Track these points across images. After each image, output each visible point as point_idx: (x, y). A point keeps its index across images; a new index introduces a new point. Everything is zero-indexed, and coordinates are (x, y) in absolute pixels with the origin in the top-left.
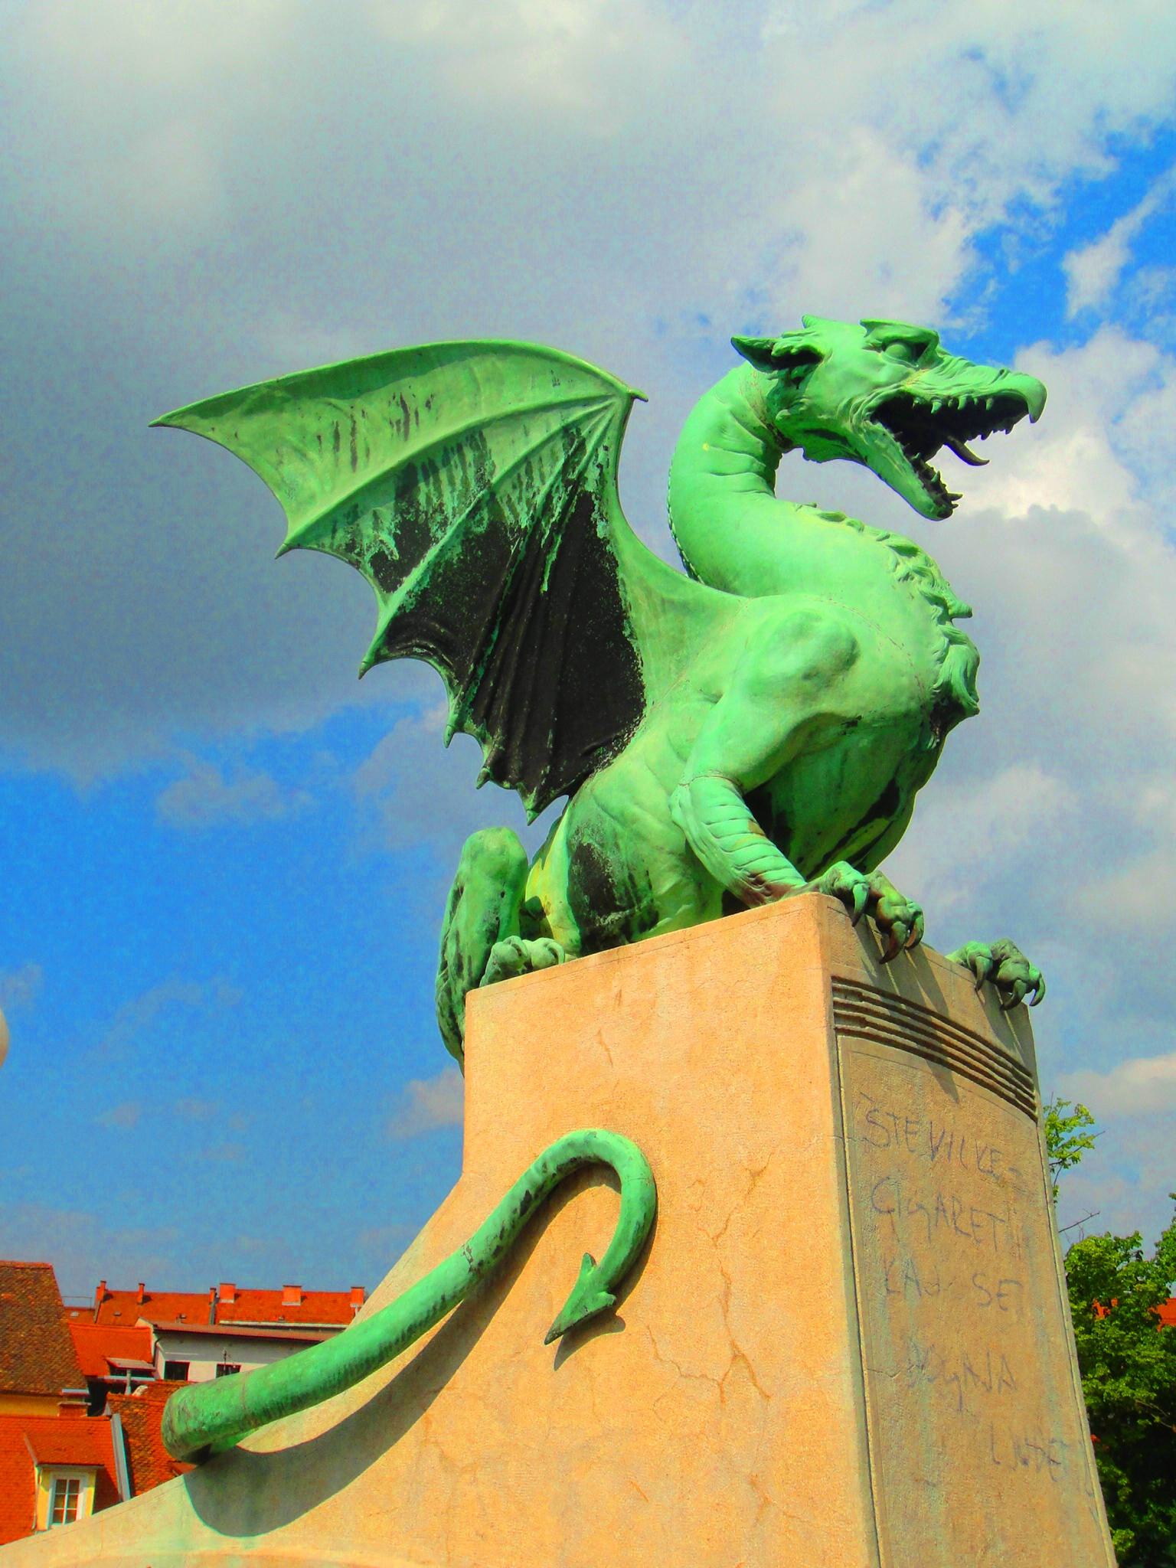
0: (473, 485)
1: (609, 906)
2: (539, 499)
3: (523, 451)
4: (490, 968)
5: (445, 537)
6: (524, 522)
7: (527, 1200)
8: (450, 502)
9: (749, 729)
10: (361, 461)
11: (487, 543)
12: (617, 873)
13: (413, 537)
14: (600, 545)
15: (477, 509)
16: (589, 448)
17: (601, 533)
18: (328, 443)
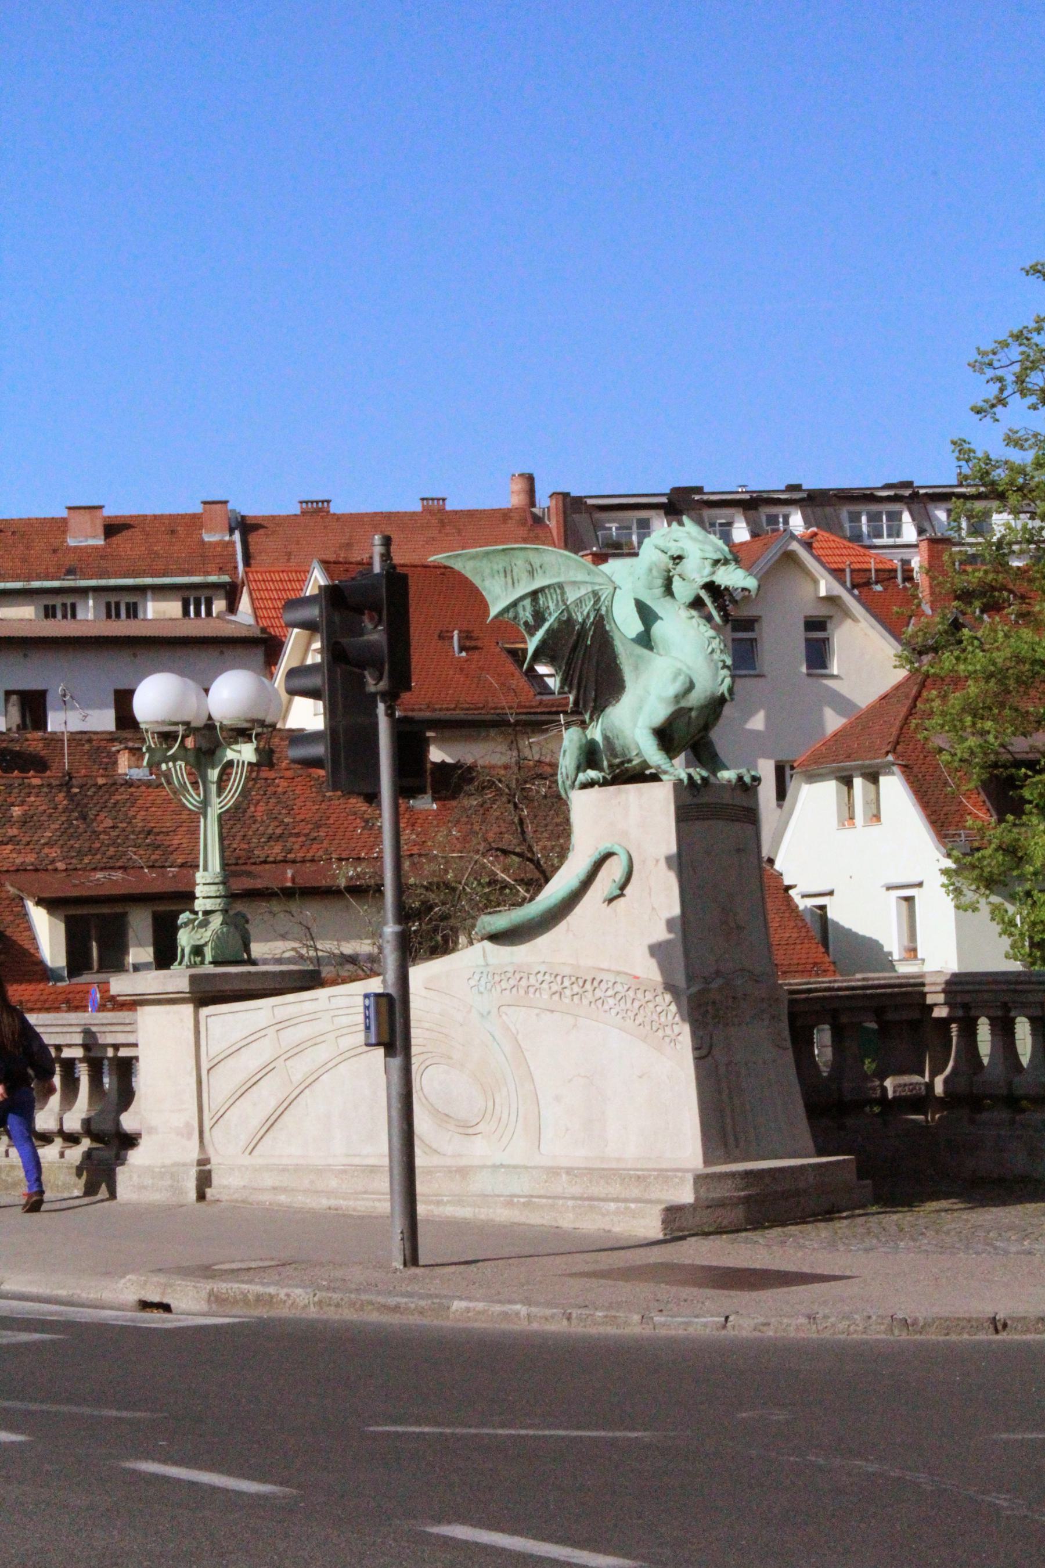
0: (560, 603)
1: (616, 756)
2: (585, 613)
3: (578, 596)
4: (577, 783)
5: (551, 620)
6: (580, 620)
7: (595, 862)
8: (552, 606)
9: (659, 713)
10: (516, 584)
11: (567, 623)
12: (619, 749)
13: (539, 617)
14: (607, 632)
15: (562, 612)
16: (602, 599)
17: (608, 628)
18: (502, 574)
